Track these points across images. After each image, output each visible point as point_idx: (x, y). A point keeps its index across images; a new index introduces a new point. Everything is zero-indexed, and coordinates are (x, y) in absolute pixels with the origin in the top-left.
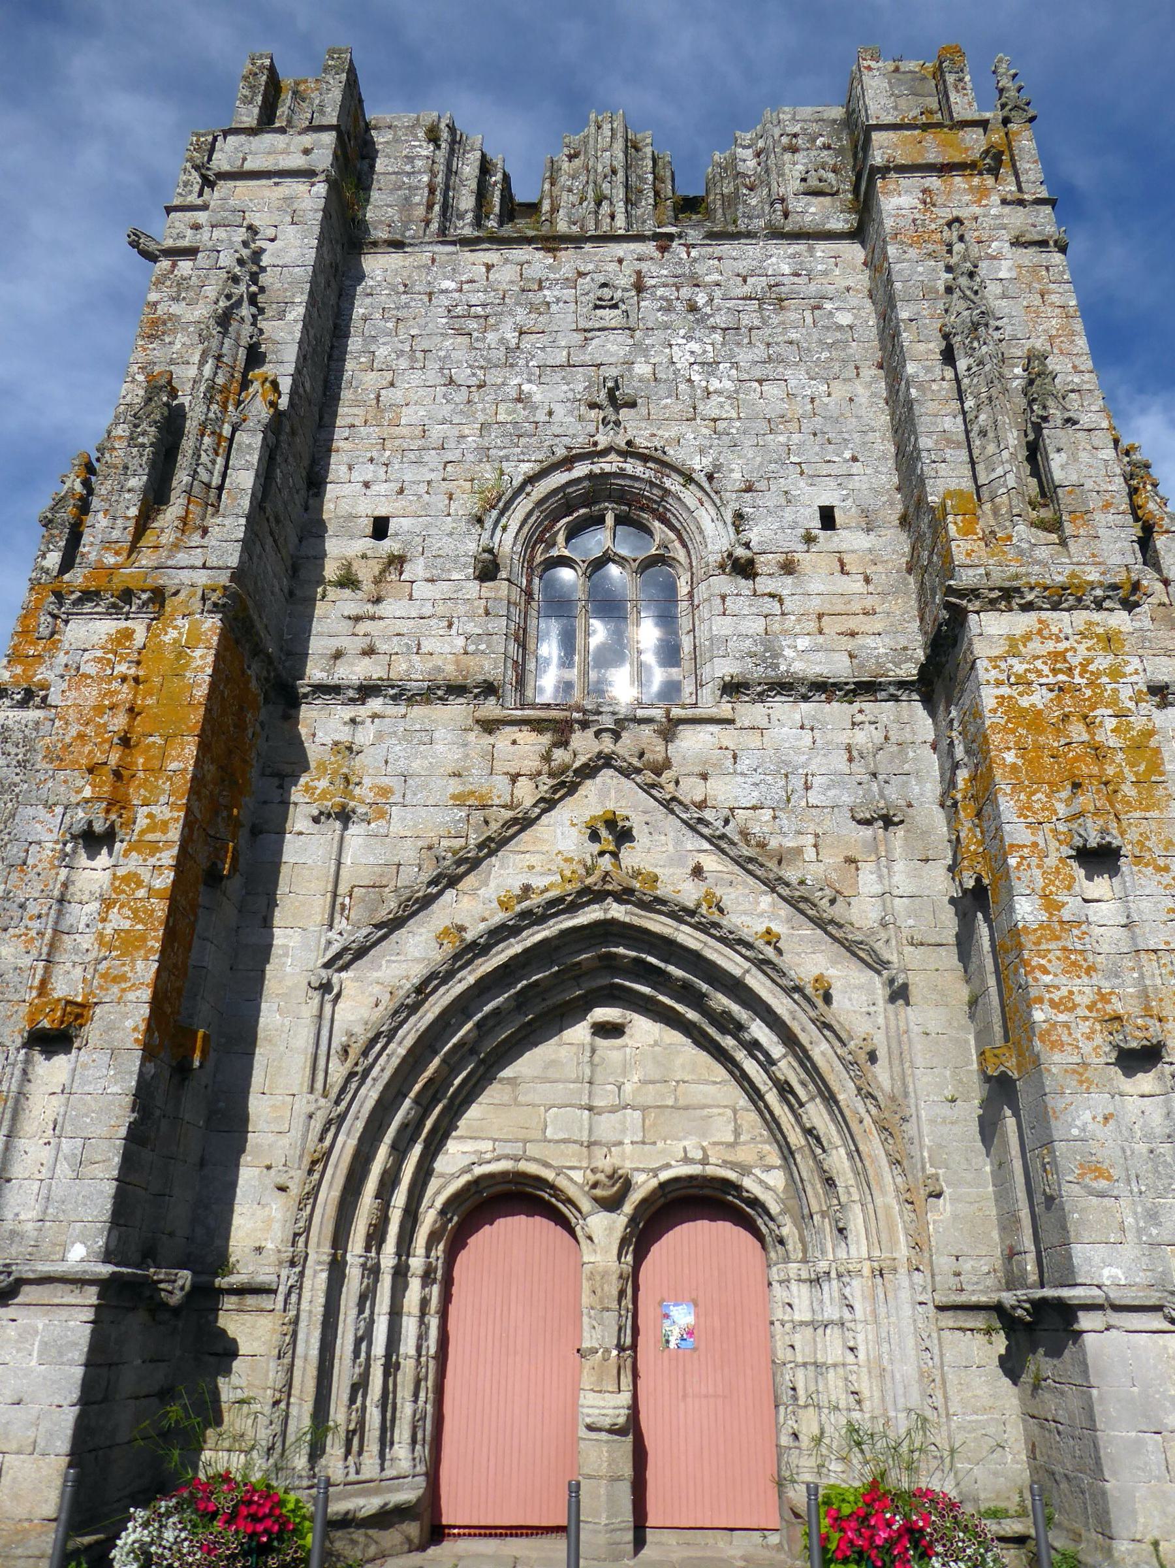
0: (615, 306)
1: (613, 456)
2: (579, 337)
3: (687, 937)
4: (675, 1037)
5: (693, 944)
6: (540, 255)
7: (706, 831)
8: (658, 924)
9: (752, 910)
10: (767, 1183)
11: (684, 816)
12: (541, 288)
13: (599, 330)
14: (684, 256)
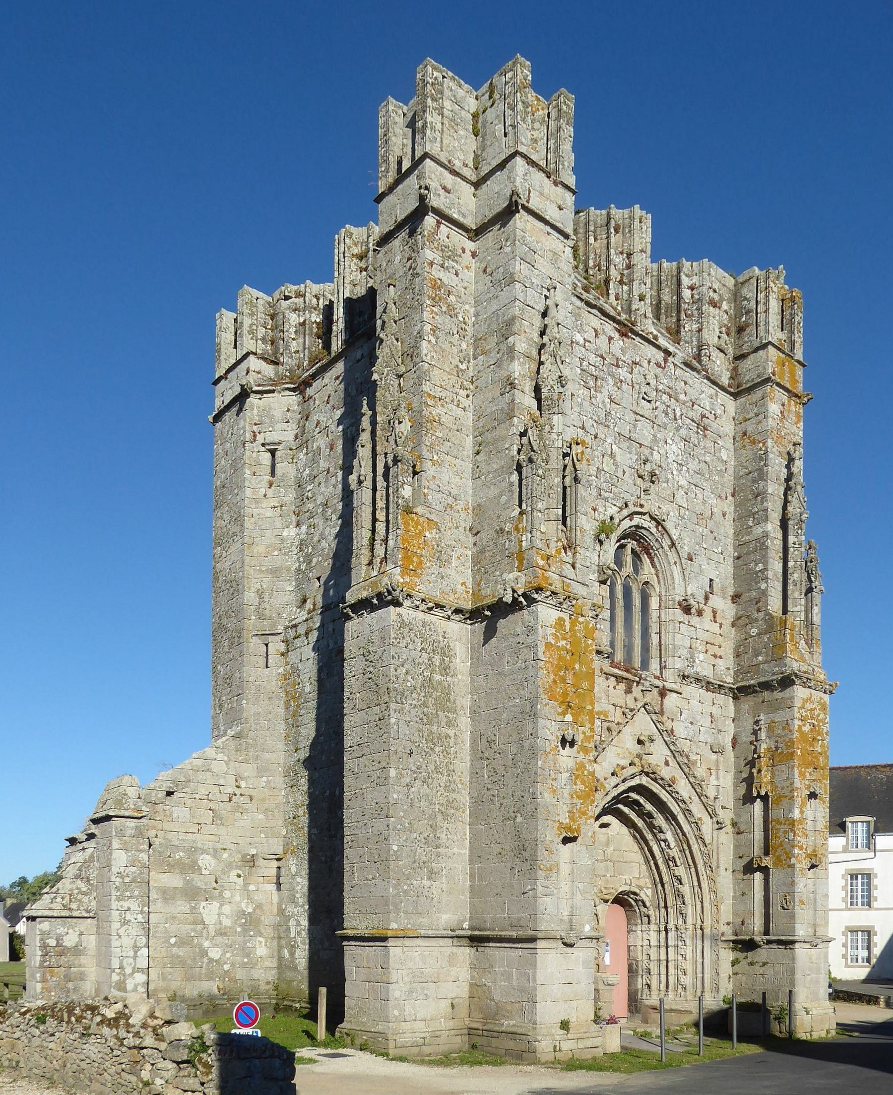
0: (649, 401)
1: (647, 517)
2: (633, 416)
3: (664, 795)
4: (624, 830)
5: (665, 799)
6: (616, 335)
7: (672, 747)
8: (655, 788)
9: (684, 788)
10: (647, 894)
11: (666, 739)
12: (618, 366)
13: (642, 416)
14: (673, 371)
